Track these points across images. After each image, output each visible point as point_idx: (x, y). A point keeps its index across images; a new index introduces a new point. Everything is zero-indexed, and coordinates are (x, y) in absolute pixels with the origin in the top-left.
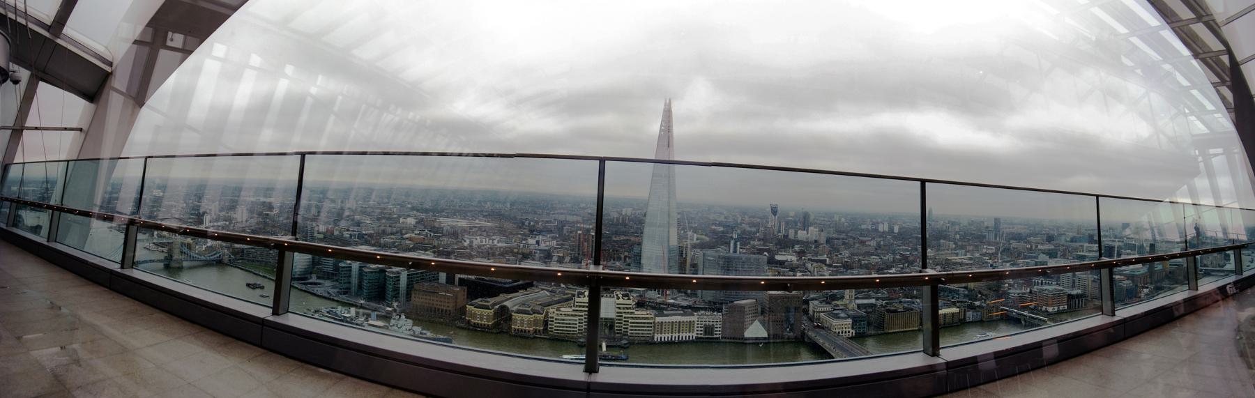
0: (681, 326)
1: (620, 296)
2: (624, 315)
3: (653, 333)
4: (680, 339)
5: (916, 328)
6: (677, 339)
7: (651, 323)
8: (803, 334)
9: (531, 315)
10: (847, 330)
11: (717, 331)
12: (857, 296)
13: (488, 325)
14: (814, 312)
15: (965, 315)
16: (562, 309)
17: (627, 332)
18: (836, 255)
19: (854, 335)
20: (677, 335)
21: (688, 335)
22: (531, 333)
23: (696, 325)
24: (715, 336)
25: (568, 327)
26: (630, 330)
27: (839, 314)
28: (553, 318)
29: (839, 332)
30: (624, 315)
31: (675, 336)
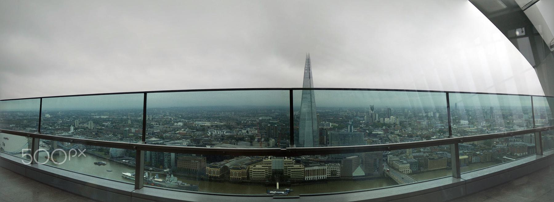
2: (288, 168)
7: (303, 171)
8: (384, 173)
9: (240, 170)
10: (407, 170)
11: (338, 173)
14: (390, 161)
16: (257, 166)
19: (411, 172)
22: (241, 179)
23: (327, 171)
27: (403, 161)
28: (252, 171)
29: (403, 171)
30: (288, 168)
31: (316, 177)
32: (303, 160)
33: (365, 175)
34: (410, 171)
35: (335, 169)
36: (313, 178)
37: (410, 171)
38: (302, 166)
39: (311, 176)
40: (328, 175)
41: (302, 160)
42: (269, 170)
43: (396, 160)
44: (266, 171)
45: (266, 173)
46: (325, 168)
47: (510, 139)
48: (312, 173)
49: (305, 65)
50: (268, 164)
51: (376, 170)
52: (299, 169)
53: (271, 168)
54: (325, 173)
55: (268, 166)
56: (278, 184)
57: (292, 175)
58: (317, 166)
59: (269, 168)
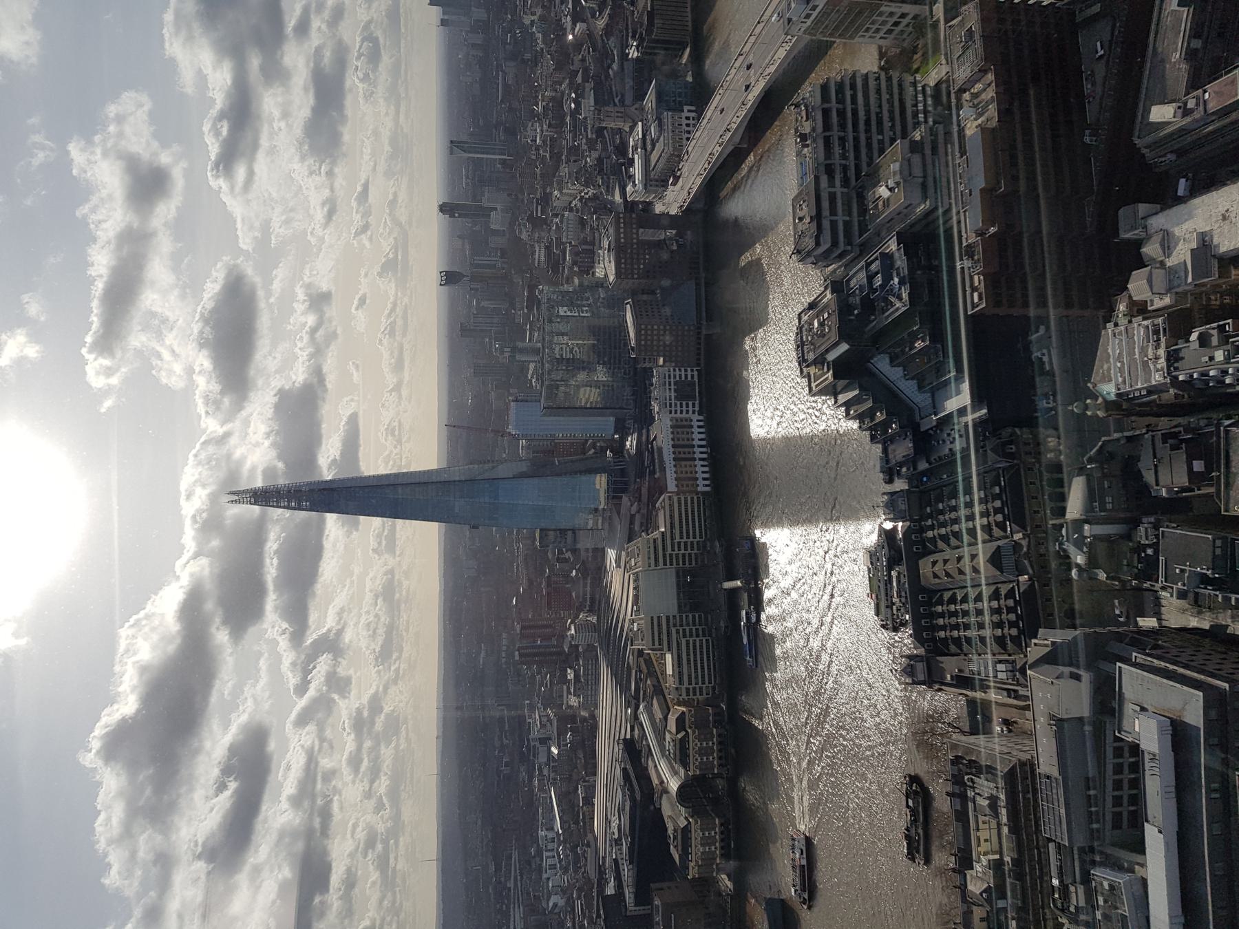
0: (681, 442)
2: (669, 551)
3: (697, 493)
4: (704, 443)
11: (686, 376)
12: (616, 100)
13: (722, 825)
19: (693, 108)
20: (697, 450)
23: (679, 415)
26: (695, 538)
28: (688, 689)
30: (669, 551)
34: (689, 111)
35: (670, 385)
36: (702, 463)
37: (689, 111)
40: (690, 409)
49: (280, 507)
54: (686, 420)
56: (728, 585)
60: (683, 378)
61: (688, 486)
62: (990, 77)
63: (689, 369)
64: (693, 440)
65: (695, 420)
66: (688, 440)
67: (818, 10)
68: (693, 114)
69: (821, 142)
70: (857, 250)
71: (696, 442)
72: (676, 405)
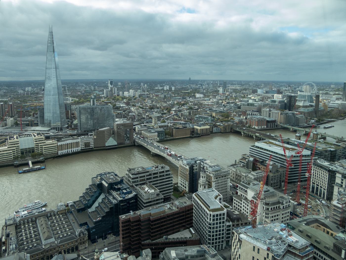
1: (36, 135)
3: (58, 151)
4: (73, 151)
5: (189, 136)
6: (71, 152)
8: (134, 141)
11: (91, 145)
14: (138, 131)
15: (212, 129)
17: (43, 153)
18: (145, 103)
21: (76, 149)
23: (80, 144)
24: (91, 147)
25: (7, 157)
29: (151, 139)
30: (40, 145)
31: (70, 151)
32: (52, 136)
33: (118, 145)
38: (55, 141)
39: (65, 150)
40: (82, 147)
41: (50, 136)
42: (16, 150)
43: (144, 130)
44: (13, 152)
45: (13, 153)
46: (79, 141)
47: (247, 113)
48: (66, 147)
50: (14, 144)
51: (127, 139)
52: (52, 144)
53: (19, 148)
55: (15, 147)
57: (45, 151)
58: (71, 139)
59: (16, 148)
60: (91, 144)
61: (60, 148)
62: (177, 210)
63: (93, 145)
64: (73, 148)
65: (79, 148)
66: (73, 147)
67: (185, 167)
68: (157, 140)
69: (156, 172)
70: (131, 185)
71: (73, 149)
72: (83, 143)
